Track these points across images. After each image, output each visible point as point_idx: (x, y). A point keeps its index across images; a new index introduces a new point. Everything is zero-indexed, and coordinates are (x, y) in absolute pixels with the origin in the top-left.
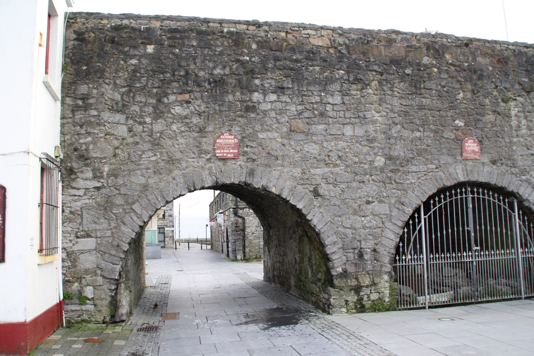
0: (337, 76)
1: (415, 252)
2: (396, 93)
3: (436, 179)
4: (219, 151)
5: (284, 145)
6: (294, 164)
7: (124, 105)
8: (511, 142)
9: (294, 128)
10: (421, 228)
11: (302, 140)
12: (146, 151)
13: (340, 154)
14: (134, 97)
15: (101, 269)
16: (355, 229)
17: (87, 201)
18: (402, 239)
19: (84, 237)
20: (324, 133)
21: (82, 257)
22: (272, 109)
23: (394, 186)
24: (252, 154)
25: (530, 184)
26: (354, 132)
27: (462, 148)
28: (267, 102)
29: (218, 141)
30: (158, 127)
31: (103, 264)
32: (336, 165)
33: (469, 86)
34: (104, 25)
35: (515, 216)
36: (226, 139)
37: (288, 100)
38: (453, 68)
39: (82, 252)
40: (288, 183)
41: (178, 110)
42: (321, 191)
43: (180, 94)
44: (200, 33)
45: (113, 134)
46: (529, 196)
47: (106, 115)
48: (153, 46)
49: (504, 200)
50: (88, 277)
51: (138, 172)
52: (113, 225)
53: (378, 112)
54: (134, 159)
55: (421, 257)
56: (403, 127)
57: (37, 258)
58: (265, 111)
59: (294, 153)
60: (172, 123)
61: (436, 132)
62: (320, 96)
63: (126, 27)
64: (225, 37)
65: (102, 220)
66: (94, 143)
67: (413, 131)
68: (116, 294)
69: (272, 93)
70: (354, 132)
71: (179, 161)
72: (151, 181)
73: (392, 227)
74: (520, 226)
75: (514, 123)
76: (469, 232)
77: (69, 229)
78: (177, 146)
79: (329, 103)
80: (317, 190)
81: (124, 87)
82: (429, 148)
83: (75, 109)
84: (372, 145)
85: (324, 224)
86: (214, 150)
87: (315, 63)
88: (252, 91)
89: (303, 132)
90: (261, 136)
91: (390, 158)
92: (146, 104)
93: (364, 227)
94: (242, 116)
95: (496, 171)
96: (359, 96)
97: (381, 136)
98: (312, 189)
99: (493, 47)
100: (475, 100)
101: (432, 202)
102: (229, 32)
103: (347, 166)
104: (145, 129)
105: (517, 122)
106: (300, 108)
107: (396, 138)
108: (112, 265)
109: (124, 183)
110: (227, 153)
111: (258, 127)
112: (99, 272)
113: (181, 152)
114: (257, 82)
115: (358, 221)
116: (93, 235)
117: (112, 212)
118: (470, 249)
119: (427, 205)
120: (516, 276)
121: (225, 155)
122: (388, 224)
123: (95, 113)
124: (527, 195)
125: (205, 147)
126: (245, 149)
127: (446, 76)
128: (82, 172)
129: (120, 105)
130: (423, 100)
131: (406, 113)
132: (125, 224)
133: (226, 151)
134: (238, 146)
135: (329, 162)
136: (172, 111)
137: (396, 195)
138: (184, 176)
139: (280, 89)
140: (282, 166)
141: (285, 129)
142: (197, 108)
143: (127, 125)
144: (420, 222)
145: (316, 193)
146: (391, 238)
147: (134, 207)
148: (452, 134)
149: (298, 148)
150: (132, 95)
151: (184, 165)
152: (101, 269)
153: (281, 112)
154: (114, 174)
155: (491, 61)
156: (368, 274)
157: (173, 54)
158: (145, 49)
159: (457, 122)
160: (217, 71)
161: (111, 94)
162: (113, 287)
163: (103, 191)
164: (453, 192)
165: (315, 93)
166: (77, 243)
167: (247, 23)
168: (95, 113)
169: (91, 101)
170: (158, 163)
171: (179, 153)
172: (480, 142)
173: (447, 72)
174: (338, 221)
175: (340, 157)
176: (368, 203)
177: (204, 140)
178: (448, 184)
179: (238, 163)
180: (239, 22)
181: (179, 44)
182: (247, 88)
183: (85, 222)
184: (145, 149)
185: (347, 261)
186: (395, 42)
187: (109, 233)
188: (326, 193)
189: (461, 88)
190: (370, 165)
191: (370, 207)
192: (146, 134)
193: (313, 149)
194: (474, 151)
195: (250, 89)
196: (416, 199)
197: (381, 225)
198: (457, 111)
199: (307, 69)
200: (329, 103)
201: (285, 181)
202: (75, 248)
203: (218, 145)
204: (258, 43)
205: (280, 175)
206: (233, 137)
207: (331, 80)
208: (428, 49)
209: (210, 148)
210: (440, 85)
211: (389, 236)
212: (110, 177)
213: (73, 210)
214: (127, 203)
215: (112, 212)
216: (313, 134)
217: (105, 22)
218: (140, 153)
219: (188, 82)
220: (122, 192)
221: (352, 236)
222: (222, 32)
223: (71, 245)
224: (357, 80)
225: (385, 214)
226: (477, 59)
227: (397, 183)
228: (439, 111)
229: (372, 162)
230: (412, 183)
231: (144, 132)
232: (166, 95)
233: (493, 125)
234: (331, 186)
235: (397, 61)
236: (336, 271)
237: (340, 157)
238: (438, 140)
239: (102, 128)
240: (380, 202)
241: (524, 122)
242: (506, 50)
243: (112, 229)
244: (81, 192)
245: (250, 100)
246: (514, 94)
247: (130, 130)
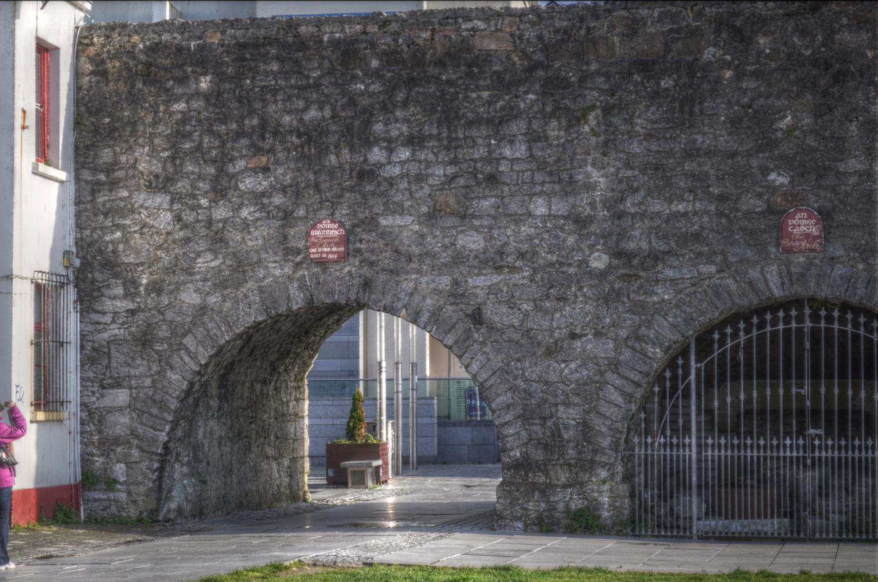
1: (675, 431)
2: (638, 128)
3: (717, 295)
4: (314, 250)
6: (441, 269)
9: (441, 205)
10: (688, 387)
11: (454, 227)
12: (202, 252)
15: (137, 437)
16: (547, 383)
17: (117, 332)
20: (493, 212)
24: (368, 254)
26: (550, 209)
27: (780, 230)
29: (312, 233)
30: (221, 213)
32: (513, 269)
36: (325, 229)
37: (431, 157)
40: (429, 301)
45: (153, 226)
51: (190, 285)
52: (155, 368)
55: (687, 441)
58: (391, 178)
67: (670, 202)
70: (550, 209)
79: (504, 158)
85: (491, 372)
90: (383, 222)
97: (603, 213)
101: (716, 336)
103: (535, 270)
106: (450, 170)
107: (634, 216)
108: (153, 431)
110: (327, 253)
117: (153, 350)
118: (801, 432)
119: (704, 342)
121: (324, 255)
122: (609, 376)
123: (125, 194)
125: (292, 244)
126: (358, 245)
132: (172, 368)
133: (325, 250)
134: (345, 240)
135: (502, 263)
138: (261, 290)
139: (414, 141)
144: (686, 374)
147: (185, 341)
152: (137, 437)
153: (420, 178)
154: (156, 288)
159: (773, 176)
163: (141, 316)
165: (480, 141)
166: (103, 396)
169: (120, 174)
174: (516, 368)
175: (521, 255)
176: (573, 336)
183: (114, 364)
184: (202, 249)
185: (530, 440)
187: (148, 382)
190: (579, 266)
192: (202, 224)
193: (472, 242)
196: (667, 331)
200: (504, 158)
201: (424, 298)
203: (313, 239)
205: (415, 289)
206: (336, 226)
209: (301, 245)
210: (738, 103)
211: (613, 398)
212: (149, 295)
213: (96, 345)
215: (153, 350)
216: (474, 216)
218: (192, 255)
221: (541, 395)
229: (584, 262)
231: (198, 221)
239: (137, 216)
243: (152, 375)
244: (108, 319)
247: (178, 219)
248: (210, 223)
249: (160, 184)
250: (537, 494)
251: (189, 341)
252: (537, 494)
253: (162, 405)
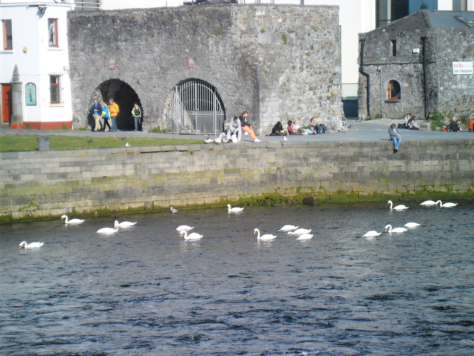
6: (131, 71)
8: (209, 58)
28: (122, 45)
32: (144, 71)
41: (98, 50)
42: (140, 82)
61: (178, 55)
91: (161, 68)
103: (147, 72)
122: (161, 96)
134: (115, 64)
139: (126, 40)
145: (138, 83)
154: (83, 75)
159: (186, 50)
160: (108, 34)
176: (154, 87)
191: (155, 89)
204: (120, 20)
207: (141, 35)
232: (94, 44)
247: (86, 58)
249: (83, 50)
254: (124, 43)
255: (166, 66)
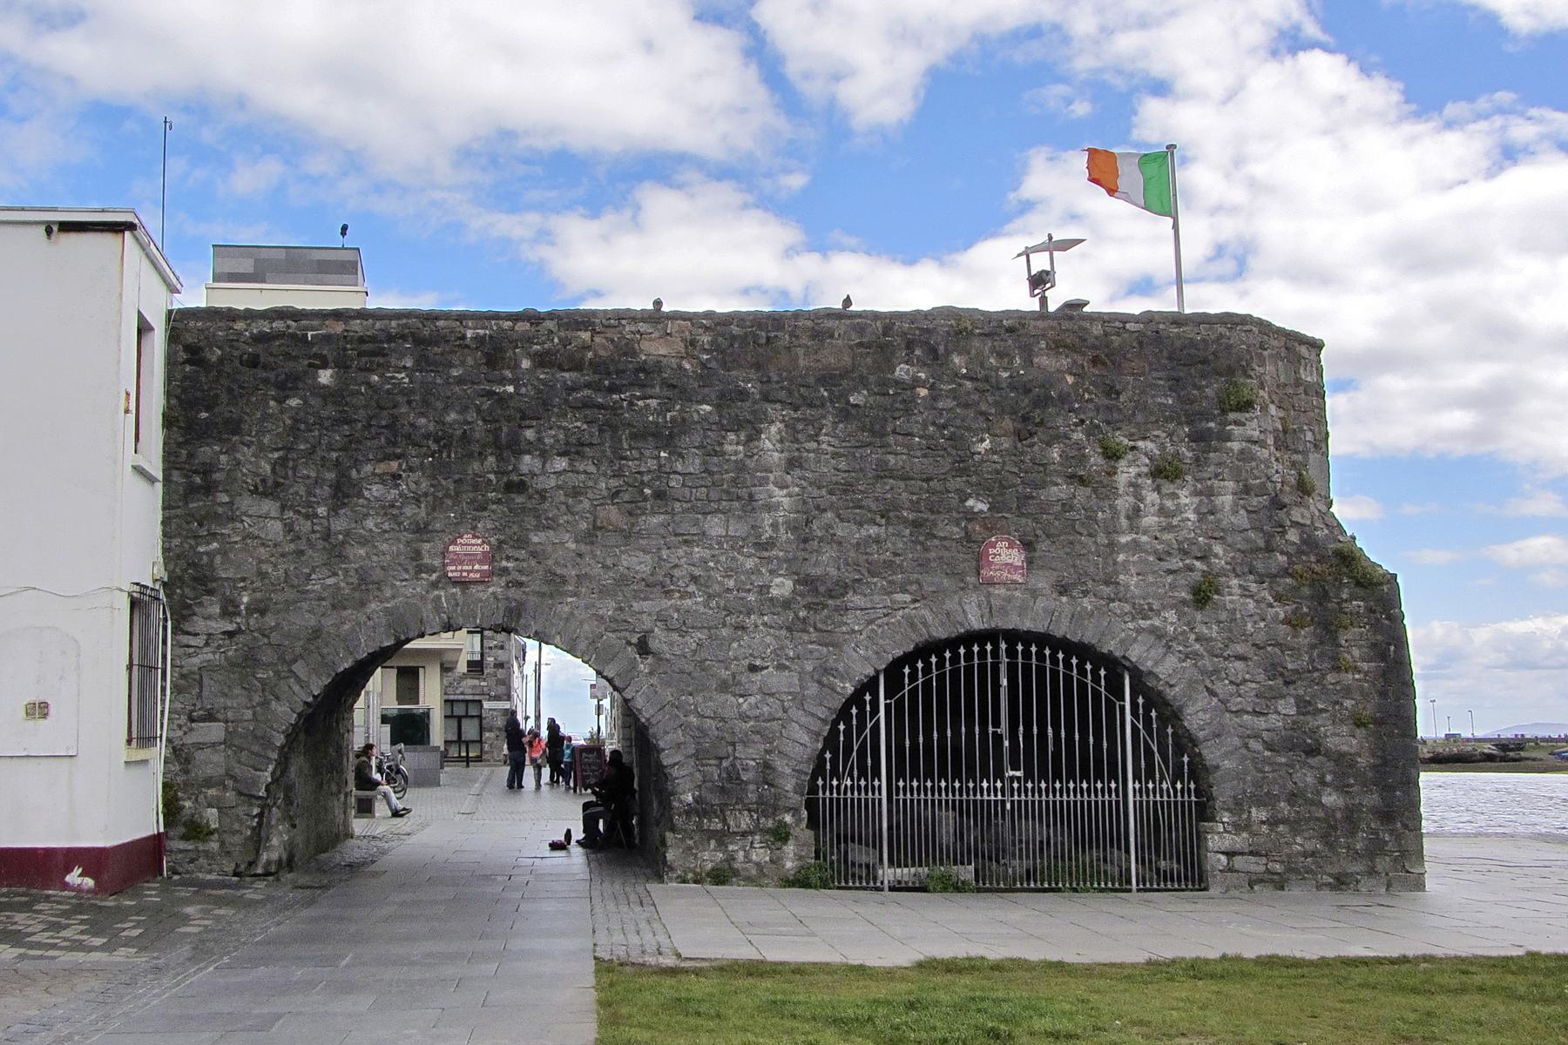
0: (696, 417)
1: (863, 773)
2: (824, 446)
3: (912, 625)
5: (580, 555)
6: (604, 592)
7: (277, 484)
8: (1111, 545)
10: (876, 726)
13: (697, 572)
14: (294, 469)
15: (232, 777)
16: (723, 720)
17: (210, 656)
18: (831, 741)
19: (204, 720)
20: (662, 531)
21: (200, 756)
22: (559, 487)
23: (814, 636)
25: (1160, 637)
28: (549, 471)
31: (238, 770)
32: (685, 595)
33: (1008, 423)
34: (240, 334)
35: (1122, 709)
37: (592, 469)
38: (969, 384)
39: (200, 746)
41: (376, 490)
42: (654, 644)
43: (381, 461)
44: (419, 341)
46: (1156, 663)
47: (246, 503)
48: (329, 372)
49: (1095, 672)
50: (212, 792)
51: (305, 605)
52: (257, 699)
53: (781, 488)
54: (296, 582)
55: (876, 783)
56: (839, 516)
57: (123, 753)
58: (545, 490)
59: (601, 571)
60: (367, 515)
61: (916, 524)
62: (658, 457)
63: (279, 335)
64: (467, 346)
65: (237, 691)
66: (224, 553)
67: (861, 524)
68: (260, 824)
69: (559, 455)
71: (379, 584)
72: (328, 622)
73: (803, 720)
74: (1135, 729)
75: (1124, 503)
76: (998, 739)
77: (179, 706)
78: (375, 558)
79: (675, 472)
80: (646, 644)
81: (277, 450)
82: (898, 560)
83: (191, 491)
84: (766, 554)
86: (444, 565)
87: (649, 391)
88: (519, 453)
89: (618, 530)
90: (535, 539)
92: (318, 481)
93: (744, 717)
94: (498, 502)
95: (1068, 610)
96: (741, 456)
97: (785, 536)
98: (634, 640)
99: (1081, 328)
100: (1022, 453)
101: (907, 670)
102: (476, 338)
103: (710, 596)
104: (317, 528)
105: (1131, 499)
106: (614, 483)
107: (821, 540)
109: (278, 624)
110: (469, 572)
111: (530, 522)
112: (229, 783)
113: (383, 568)
114: (530, 434)
115: (731, 704)
116: (220, 716)
118: (999, 774)
119: (893, 672)
120: (1121, 841)
122: (795, 713)
123: (226, 499)
124: (1149, 663)
125: (427, 560)
126: (504, 563)
127: (950, 403)
128: (201, 604)
129: (270, 482)
130: (891, 458)
131: (847, 488)
132: (278, 698)
134: (489, 558)
136: (366, 493)
137: (816, 654)
139: (575, 449)
140: (575, 594)
141: (584, 526)
142: (413, 486)
143: (282, 520)
144: (875, 710)
145: (643, 648)
146: (800, 741)
147: (294, 668)
148: (956, 529)
149: (609, 562)
150: (291, 464)
151: (388, 593)
152: (232, 777)
153: (576, 493)
154: (259, 609)
155: (1075, 362)
156: (749, 810)
157: (368, 384)
158: (316, 376)
161: (256, 462)
162: (256, 811)
163: (241, 638)
164: (962, 651)
165: (647, 453)
166: (191, 730)
167: (515, 317)
168: (226, 499)
169: (217, 476)
170: (339, 588)
171: (378, 571)
172: (1028, 546)
173: (954, 394)
175: (694, 579)
176: (753, 669)
177: (427, 546)
178: (941, 633)
179: (491, 590)
180: (497, 316)
181: (379, 365)
182: (509, 447)
183: (206, 693)
186: (832, 336)
187: (248, 714)
188: (665, 648)
189: (988, 430)
190: (760, 593)
193: (638, 563)
194: (1010, 567)
195: (515, 447)
197: (780, 714)
198: (974, 479)
199: (631, 404)
200: (675, 472)
201: (581, 623)
202: (189, 740)
207: (683, 426)
208: (910, 346)
209: (437, 563)
211: (797, 736)
213: (185, 671)
214: (282, 659)
217: (240, 325)
219: (396, 440)
220: (273, 641)
222: (464, 337)
223: (180, 733)
224: (737, 425)
225: (789, 693)
226: (1036, 360)
227: (822, 631)
228: (928, 480)
229: (764, 589)
230: (853, 631)
231: (314, 532)
232: (357, 464)
233: (1067, 506)
234: (675, 636)
235: (832, 377)
236: (681, 802)
237: (694, 579)
238: (921, 543)
239: (238, 525)
240: (781, 667)
241: (1152, 497)
242: (1118, 334)
244: (199, 641)
245: (515, 469)
246: (1132, 435)
247: (289, 528)
248: (327, 535)
249: (267, 489)
250: (713, 843)
251: (299, 668)
252: (713, 843)
253: (267, 742)
254: (561, 464)
255: (833, 572)
